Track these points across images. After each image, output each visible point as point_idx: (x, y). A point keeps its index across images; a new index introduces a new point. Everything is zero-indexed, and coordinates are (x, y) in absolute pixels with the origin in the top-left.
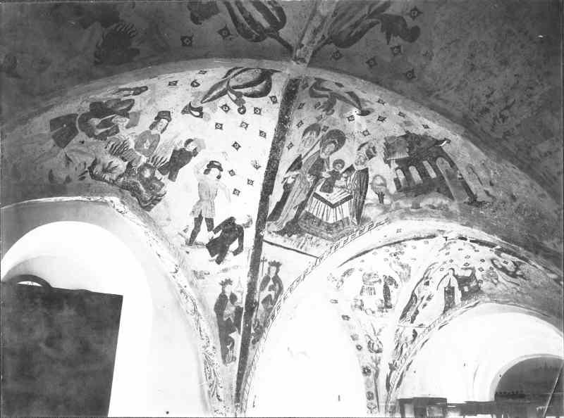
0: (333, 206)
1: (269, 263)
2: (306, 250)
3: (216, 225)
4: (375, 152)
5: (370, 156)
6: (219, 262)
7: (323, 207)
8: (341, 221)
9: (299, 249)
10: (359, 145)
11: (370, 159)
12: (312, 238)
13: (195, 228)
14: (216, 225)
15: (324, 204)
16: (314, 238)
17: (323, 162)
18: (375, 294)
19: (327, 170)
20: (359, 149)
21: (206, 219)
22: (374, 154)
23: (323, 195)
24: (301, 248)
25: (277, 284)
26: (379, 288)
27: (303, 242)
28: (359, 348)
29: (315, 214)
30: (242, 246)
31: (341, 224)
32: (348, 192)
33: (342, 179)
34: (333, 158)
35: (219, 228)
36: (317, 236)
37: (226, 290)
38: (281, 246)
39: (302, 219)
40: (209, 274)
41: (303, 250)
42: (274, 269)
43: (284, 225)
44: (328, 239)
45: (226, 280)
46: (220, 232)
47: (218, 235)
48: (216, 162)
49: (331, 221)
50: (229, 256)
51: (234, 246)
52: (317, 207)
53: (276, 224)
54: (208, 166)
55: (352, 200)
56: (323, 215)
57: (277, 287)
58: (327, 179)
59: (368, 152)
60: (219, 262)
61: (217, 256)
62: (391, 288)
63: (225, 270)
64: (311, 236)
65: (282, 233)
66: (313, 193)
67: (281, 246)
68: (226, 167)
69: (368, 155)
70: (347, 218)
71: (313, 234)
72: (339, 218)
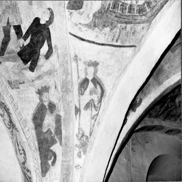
1: (85, 63)
2: (122, 42)
3: (24, 32)
6: (32, 69)
9: (115, 43)
12: (126, 28)
13: (5, 36)
14: (24, 32)
16: (129, 26)
24: (117, 41)
25: (98, 87)
27: (117, 34)
36: (131, 23)
37: (44, 99)
38: (94, 42)
39: (110, 9)
40: (24, 83)
41: (119, 43)
42: (91, 69)
44: (144, 22)
45: (42, 87)
46: (29, 38)
47: (28, 41)
50: (42, 61)
51: (44, 49)
57: (99, 90)
60: (32, 69)
61: (29, 63)
63: (39, 77)
64: (124, 25)
65: (93, 25)
67: (94, 42)
71: (126, 23)
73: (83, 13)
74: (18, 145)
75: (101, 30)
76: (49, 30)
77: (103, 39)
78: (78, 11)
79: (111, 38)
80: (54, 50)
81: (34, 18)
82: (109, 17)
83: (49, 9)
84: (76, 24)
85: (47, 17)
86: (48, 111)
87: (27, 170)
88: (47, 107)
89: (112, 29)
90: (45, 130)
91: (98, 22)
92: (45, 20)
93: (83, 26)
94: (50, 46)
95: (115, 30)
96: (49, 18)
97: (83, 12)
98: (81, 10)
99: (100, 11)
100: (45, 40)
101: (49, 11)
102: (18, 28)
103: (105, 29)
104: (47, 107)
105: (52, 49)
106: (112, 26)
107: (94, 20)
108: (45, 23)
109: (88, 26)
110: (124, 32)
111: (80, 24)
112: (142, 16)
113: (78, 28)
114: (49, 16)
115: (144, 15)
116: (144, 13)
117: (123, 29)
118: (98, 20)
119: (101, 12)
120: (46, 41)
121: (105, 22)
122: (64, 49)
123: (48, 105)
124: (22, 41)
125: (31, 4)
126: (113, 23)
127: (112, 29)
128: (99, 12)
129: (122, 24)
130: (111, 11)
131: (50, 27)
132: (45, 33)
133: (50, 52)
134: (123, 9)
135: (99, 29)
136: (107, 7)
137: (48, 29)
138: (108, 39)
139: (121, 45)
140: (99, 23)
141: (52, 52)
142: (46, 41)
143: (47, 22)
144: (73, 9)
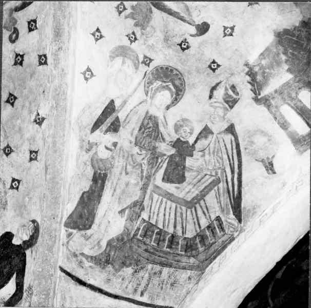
2: (151, 297)
4: (237, 94)
5: (231, 102)
8: (209, 227)
9: (138, 298)
10: (210, 89)
11: (231, 107)
12: (161, 272)
15: (174, 205)
16: (166, 270)
20: (210, 97)
22: (235, 96)
23: (171, 188)
24: (142, 294)
31: (208, 233)
32: (211, 176)
33: (197, 154)
34: (173, 116)
36: (171, 266)
38: (100, 291)
39: (138, 237)
44: (191, 268)
52: (162, 210)
53: (87, 238)
55: (221, 185)
56: (175, 227)
58: (171, 157)
64: (157, 268)
65: (103, 261)
66: (150, 187)
67: (100, 291)
69: (227, 102)
70: (218, 219)
71: (163, 264)
72: (204, 222)
73: (90, 237)
75: (117, 270)
76: (25, 256)
77: (118, 286)
78: (83, 232)
79: (133, 286)
80: (25, 295)
81: (3, 232)
82: (134, 250)
83: (34, 221)
84: (74, 253)
85: (27, 235)
89: (136, 272)
91: (114, 255)
92: (22, 240)
93: (87, 259)
94: (20, 286)
95: (141, 274)
96: (31, 236)
97: (92, 235)
98: (89, 232)
99: (120, 238)
100: (14, 274)
101: (32, 225)
103: (125, 269)
105: (22, 293)
106: (137, 265)
107: (107, 252)
108: (21, 245)
109: (96, 260)
110: (156, 281)
111: (82, 254)
112: (189, 257)
113: (77, 261)
114: (31, 234)
115: (193, 256)
116: (194, 252)
117: (155, 273)
118: (115, 251)
119: (123, 239)
120: (15, 276)
121: (126, 257)
122: (44, 297)
125: (4, 209)
126: (139, 260)
127: (136, 272)
128: (118, 239)
129: (155, 266)
130: (139, 240)
131: (28, 252)
132: (16, 261)
133: (17, 297)
134: (159, 240)
135: (114, 267)
136: (133, 233)
137: (24, 255)
138: (127, 287)
139: (149, 302)
140: (115, 257)
141: (21, 298)
142: (15, 276)
143: (24, 242)
144: (74, 228)
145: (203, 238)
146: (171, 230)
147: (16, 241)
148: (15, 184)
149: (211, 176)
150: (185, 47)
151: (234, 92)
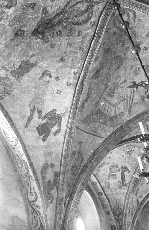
0: (114, 106)
6: (44, 140)
7: (108, 106)
8: (119, 114)
14: (43, 115)
17: (110, 76)
18: (116, 178)
19: (112, 82)
21: (38, 110)
23: (108, 98)
24: (95, 132)
26: (119, 174)
28: (108, 213)
29: (103, 111)
30: (60, 129)
35: (45, 116)
43: (86, 115)
46: (46, 120)
47: (44, 121)
48: (47, 71)
49: (113, 114)
50: (51, 136)
51: (55, 129)
54: (42, 74)
57: (81, 159)
58: (111, 88)
59: (135, 70)
60: (44, 140)
62: (126, 173)
68: (54, 76)
70: (122, 113)
74: (31, 189)
86: (50, 168)
87: (36, 206)
88: (50, 165)
90: (47, 181)
102: (40, 112)
104: (50, 165)
114: (65, 112)
123: (51, 164)
124: (40, 120)
130: (95, 115)
145: (116, 117)
146: (106, 113)
147: (58, 113)
148: (59, 92)
149: (123, 97)
150: (128, 49)
151: (139, 70)
